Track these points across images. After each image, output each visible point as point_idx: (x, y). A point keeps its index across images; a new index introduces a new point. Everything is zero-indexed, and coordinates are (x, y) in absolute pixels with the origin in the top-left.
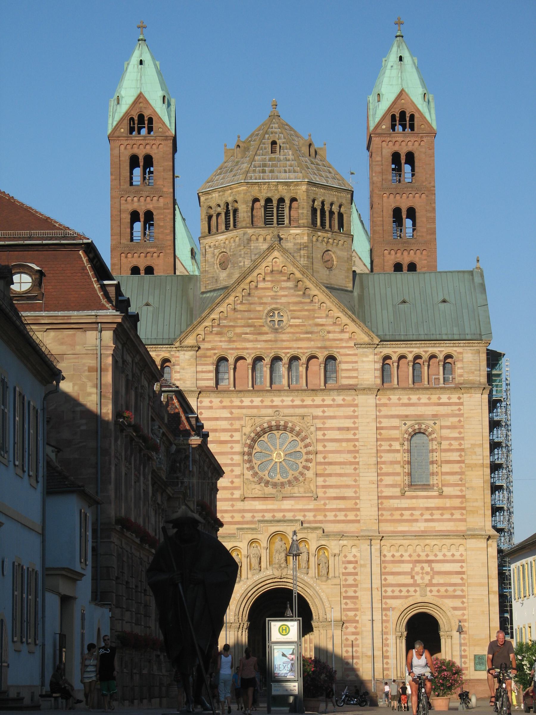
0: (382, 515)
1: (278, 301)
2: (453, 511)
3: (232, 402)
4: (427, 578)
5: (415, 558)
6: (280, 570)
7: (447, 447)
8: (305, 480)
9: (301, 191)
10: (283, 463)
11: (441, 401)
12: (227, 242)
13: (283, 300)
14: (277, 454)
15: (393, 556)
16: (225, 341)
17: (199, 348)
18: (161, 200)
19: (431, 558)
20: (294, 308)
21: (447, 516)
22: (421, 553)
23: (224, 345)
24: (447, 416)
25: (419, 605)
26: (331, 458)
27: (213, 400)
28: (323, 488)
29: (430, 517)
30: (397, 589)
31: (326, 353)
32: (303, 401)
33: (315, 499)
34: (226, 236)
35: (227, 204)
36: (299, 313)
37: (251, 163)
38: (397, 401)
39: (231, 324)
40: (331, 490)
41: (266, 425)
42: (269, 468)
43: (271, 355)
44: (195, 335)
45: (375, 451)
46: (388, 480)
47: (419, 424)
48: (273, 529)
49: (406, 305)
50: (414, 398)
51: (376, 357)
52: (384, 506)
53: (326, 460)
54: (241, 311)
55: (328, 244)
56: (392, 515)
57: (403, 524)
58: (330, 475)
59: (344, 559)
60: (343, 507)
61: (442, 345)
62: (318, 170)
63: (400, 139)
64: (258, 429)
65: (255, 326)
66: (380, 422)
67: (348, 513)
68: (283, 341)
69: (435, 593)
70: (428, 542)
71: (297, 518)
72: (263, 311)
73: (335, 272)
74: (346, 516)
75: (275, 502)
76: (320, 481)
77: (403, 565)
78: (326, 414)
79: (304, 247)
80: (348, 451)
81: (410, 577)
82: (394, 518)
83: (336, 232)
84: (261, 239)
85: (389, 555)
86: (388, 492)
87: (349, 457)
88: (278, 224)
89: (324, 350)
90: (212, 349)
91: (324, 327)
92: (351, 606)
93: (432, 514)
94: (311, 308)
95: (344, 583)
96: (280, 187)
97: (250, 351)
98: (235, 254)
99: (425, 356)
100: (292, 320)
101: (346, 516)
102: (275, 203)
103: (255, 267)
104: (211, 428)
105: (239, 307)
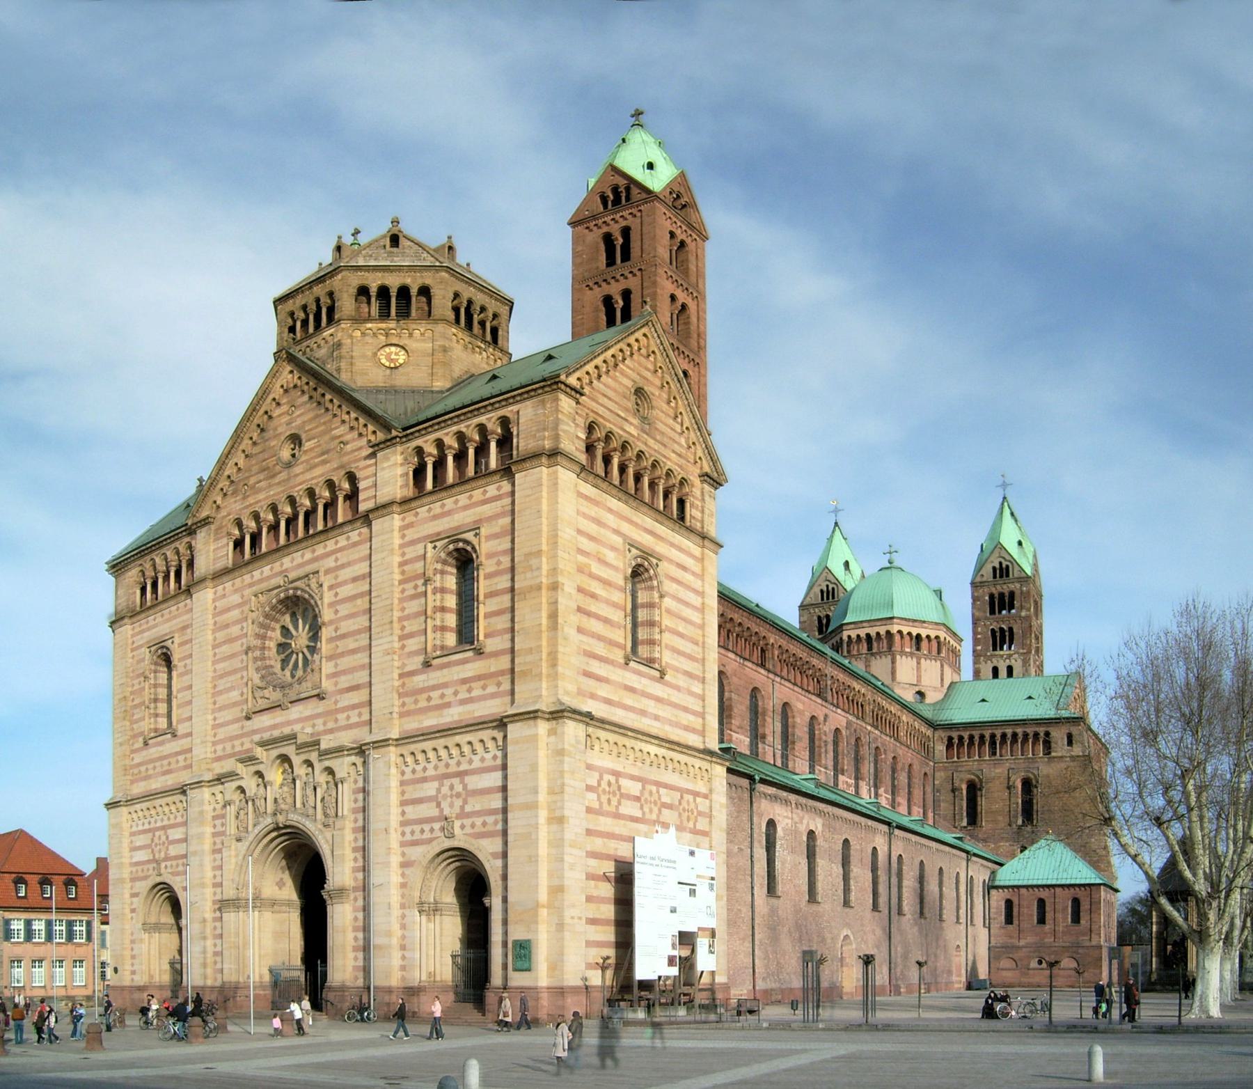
2: (500, 678)
4: (458, 803)
5: (442, 770)
11: (488, 495)
19: (464, 767)
26: (346, 626)
29: (467, 696)
33: (323, 698)
38: (427, 514)
40: (343, 678)
48: (275, 753)
50: (449, 503)
56: (416, 702)
57: (430, 714)
58: (342, 655)
69: (468, 830)
70: (458, 739)
77: (426, 785)
81: (434, 804)
85: (408, 770)
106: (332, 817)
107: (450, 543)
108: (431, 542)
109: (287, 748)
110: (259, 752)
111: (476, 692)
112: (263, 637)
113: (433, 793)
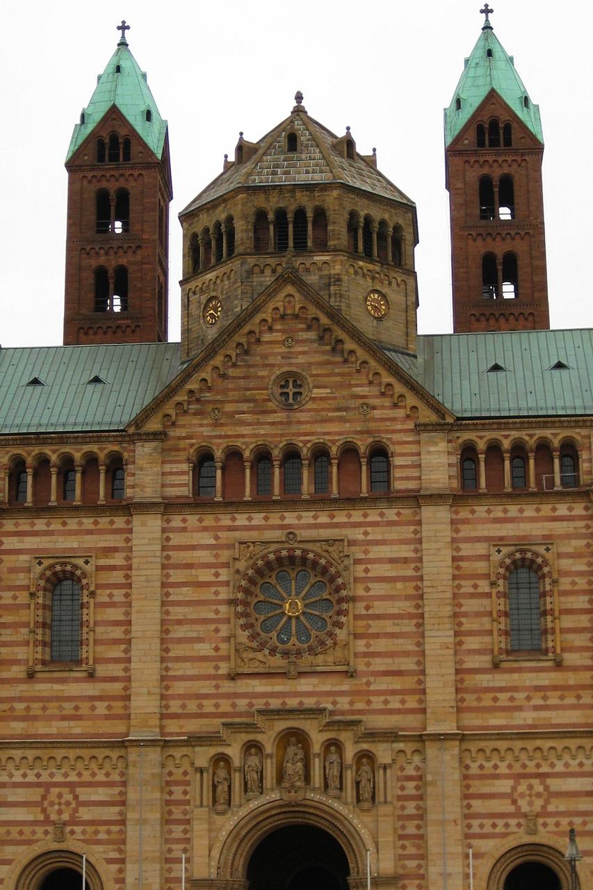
0: (463, 700)
1: (293, 361)
2: (581, 692)
3: (217, 520)
4: (539, 803)
5: (517, 769)
6: (293, 791)
7: (568, 587)
8: (335, 644)
9: (331, 200)
10: (302, 618)
11: (558, 513)
12: (218, 281)
13: (301, 360)
14: (290, 604)
15: (481, 767)
16: (208, 425)
17: (165, 434)
18: (139, 252)
20: (319, 372)
21: (570, 700)
22: (528, 763)
23: (206, 431)
24: (568, 537)
25: (525, 848)
26: (379, 608)
27: (188, 517)
28: (364, 657)
29: (542, 702)
30: (488, 822)
31: (370, 440)
32: (332, 517)
33: (352, 676)
34: (217, 271)
35: (218, 224)
36: (326, 379)
37: (257, 165)
38: (485, 515)
39: (219, 397)
40: (378, 660)
41: (272, 556)
42: (279, 628)
43: (281, 445)
44: (160, 415)
45: (449, 595)
46: (472, 643)
47: (521, 551)
48: (282, 725)
49: (501, 374)
50: (513, 510)
51: (450, 444)
52: (465, 684)
53: (370, 612)
54: (234, 378)
55: (376, 281)
56: (479, 700)
57: (498, 714)
59: (399, 773)
60: (398, 687)
61: (557, 425)
62: (360, 174)
63: (491, 159)
64: (260, 563)
65: (255, 401)
66: (458, 549)
67: (407, 698)
68: (300, 422)
69: (552, 828)
70: (539, 743)
71: (322, 706)
72: (269, 377)
73: (388, 323)
74: (403, 702)
75: (286, 681)
76: (360, 645)
77: (497, 782)
78: (369, 538)
79: (335, 282)
80: (406, 595)
81: (509, 801)
82: (482, 704)
83: (388, 264)
84: (268, 271)
86: (471, 662)
87: (407, 607)
88: (294, 247)
89: (366, 436)
90: (189, 437)
91: (366, 401)
92: (411, 850)
93: (545, 698)
94: (346, 370)
95: (400, 813)
96: (298, 194)
97: (248, 440)
98: (229, 297)
99: (532, 443)
100: (315, 391)
101: (403, 702)
102: (290, 216)
103: (257, 310)
104: (184, 562)
105: (231, 372)
106: (367, 798)
107: (517, 551)
108: (495, 545)
109: (303, 721)
110: (259, 720)
111: (553, 701)
112: (247, 592)
113: (508, 790)
